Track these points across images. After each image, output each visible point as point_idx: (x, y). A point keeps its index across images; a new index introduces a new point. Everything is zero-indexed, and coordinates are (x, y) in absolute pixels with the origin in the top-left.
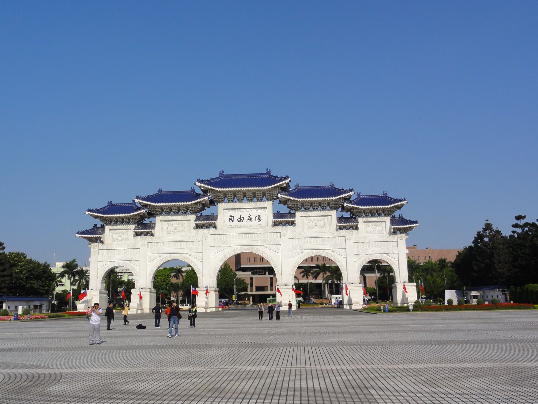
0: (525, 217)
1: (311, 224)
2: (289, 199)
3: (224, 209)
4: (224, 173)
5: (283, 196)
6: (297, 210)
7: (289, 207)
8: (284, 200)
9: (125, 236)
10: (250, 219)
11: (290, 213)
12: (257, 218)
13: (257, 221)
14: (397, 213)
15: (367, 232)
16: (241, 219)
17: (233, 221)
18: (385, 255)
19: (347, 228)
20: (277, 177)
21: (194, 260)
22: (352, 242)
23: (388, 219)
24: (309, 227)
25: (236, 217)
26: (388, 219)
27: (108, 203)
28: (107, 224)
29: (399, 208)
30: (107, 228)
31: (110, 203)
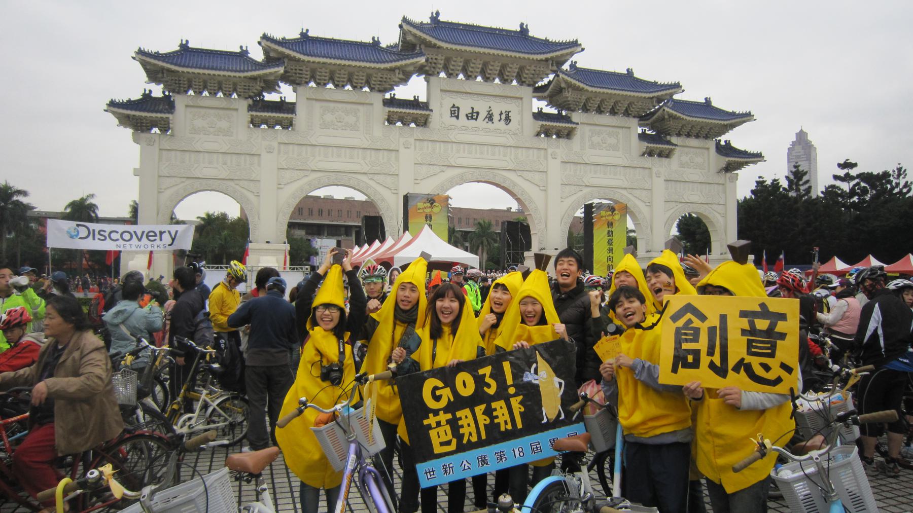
0: (855, 165)
1: (596, 139)
2: (570, 85)
3: (442, 91)
4: (442, 18)
5: (566, 77)
6: (573, 111)
7: (551, 103)
8: (563, 85)
9: (224, 124)
10: (490, 117)
11: (560, 114)
12: (503, 116)
13: (503, 122)
14: (723, 139)
15: (682, 165)
16: (473, 115)
17: (457, 117)
18: (706, 206)
19: (650, 153)
20: (547, 41)
21: (380, 189)
22: (663, 178)
23: (711, 144)
24: (593, 146)
25: (465, 110)
26: (711, 144)
27: (181, 45)
28: (179, 93)
29: (732, 126)
30: (180, 101)
31: (184, 47)
